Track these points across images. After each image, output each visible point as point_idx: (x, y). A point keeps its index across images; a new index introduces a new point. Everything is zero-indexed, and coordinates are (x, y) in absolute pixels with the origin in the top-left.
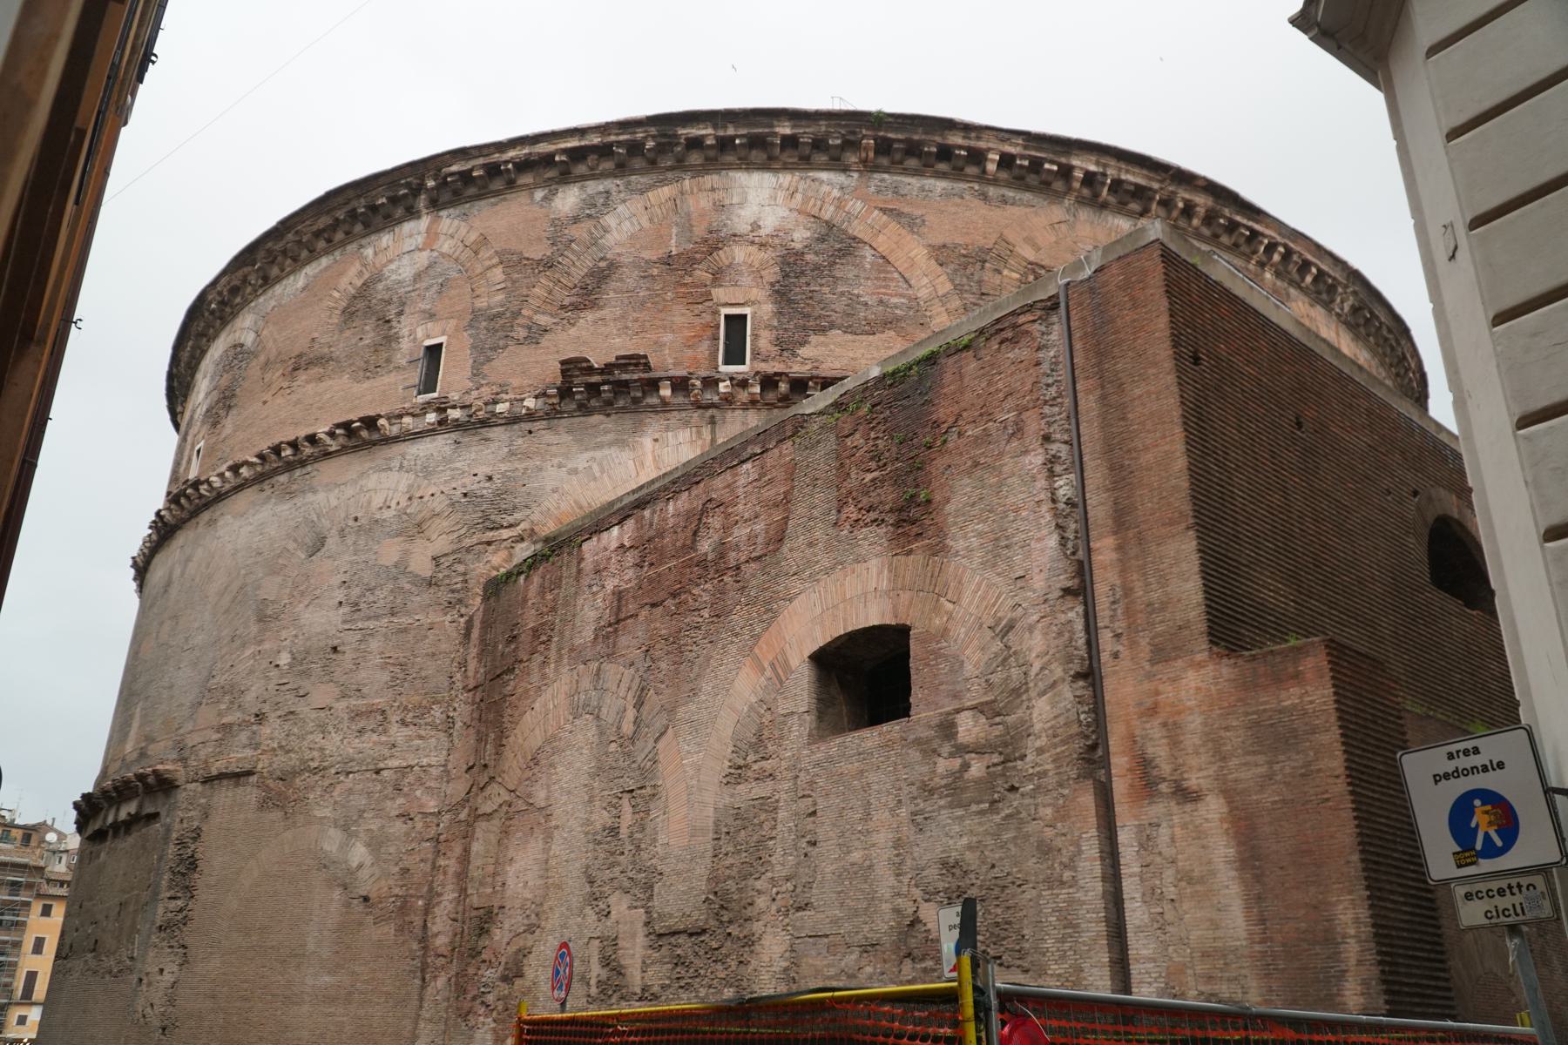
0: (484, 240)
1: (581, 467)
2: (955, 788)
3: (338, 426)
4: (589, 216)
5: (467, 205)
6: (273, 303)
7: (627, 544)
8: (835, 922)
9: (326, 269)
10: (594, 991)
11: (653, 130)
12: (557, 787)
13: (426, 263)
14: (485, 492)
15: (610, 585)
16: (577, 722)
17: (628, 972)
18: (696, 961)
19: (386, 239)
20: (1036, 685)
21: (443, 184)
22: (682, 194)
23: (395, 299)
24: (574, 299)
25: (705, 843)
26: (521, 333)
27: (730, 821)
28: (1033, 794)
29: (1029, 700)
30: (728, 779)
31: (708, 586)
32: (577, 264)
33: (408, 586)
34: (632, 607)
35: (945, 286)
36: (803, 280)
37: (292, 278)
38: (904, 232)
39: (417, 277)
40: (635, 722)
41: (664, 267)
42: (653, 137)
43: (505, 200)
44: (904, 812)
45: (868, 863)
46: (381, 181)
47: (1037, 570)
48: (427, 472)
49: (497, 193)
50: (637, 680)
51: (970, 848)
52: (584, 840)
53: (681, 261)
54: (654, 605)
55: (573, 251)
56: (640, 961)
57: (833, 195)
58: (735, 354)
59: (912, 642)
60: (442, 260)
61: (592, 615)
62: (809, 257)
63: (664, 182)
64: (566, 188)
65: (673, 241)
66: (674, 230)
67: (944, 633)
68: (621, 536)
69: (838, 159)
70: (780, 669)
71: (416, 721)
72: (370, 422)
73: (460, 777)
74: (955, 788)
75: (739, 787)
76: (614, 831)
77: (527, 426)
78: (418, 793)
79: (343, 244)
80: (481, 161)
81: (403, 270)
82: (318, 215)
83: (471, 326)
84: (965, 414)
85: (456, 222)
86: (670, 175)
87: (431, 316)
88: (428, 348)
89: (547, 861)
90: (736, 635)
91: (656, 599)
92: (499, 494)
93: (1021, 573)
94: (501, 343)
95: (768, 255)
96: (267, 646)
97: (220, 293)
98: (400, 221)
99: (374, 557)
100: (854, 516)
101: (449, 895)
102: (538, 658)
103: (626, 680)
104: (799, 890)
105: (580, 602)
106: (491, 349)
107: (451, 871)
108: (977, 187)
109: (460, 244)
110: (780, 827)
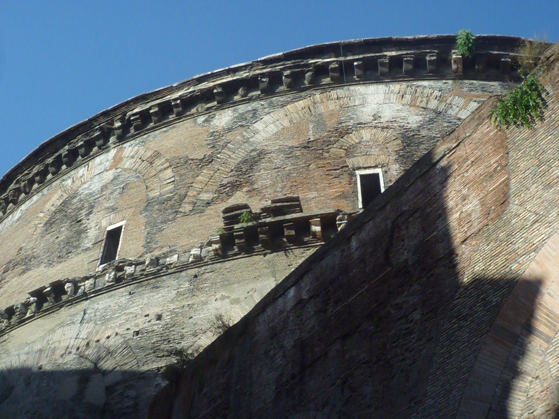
0: (157, 155)
1: (242, 297)
3: (33, 294)
7: (305, 297)
11: (289, 63)
13: (111, 177)
14: (155, 327)
15: (289, 343)
21: (127, 125)
23: (86, 205)
24: (230, 179)
26: (187, 207)
32: (233, 156)
37: (11, 216)
39: (104, 187)
41: (305, 151)
43: (174, 127)
48: (105, 320)
55: (229, 149)
62: (424, 132)
64: (222, 112)
65: (311, 132)
66: (311, 126)
68: (298, 292)
77: (193, 272)
81: (96, 186)
83: (145, 210)
85: (136, 148)
87: (113, 209)
88: (110, 232)
90: (465, 318)
106: (162, 223)
109: (139, 161)
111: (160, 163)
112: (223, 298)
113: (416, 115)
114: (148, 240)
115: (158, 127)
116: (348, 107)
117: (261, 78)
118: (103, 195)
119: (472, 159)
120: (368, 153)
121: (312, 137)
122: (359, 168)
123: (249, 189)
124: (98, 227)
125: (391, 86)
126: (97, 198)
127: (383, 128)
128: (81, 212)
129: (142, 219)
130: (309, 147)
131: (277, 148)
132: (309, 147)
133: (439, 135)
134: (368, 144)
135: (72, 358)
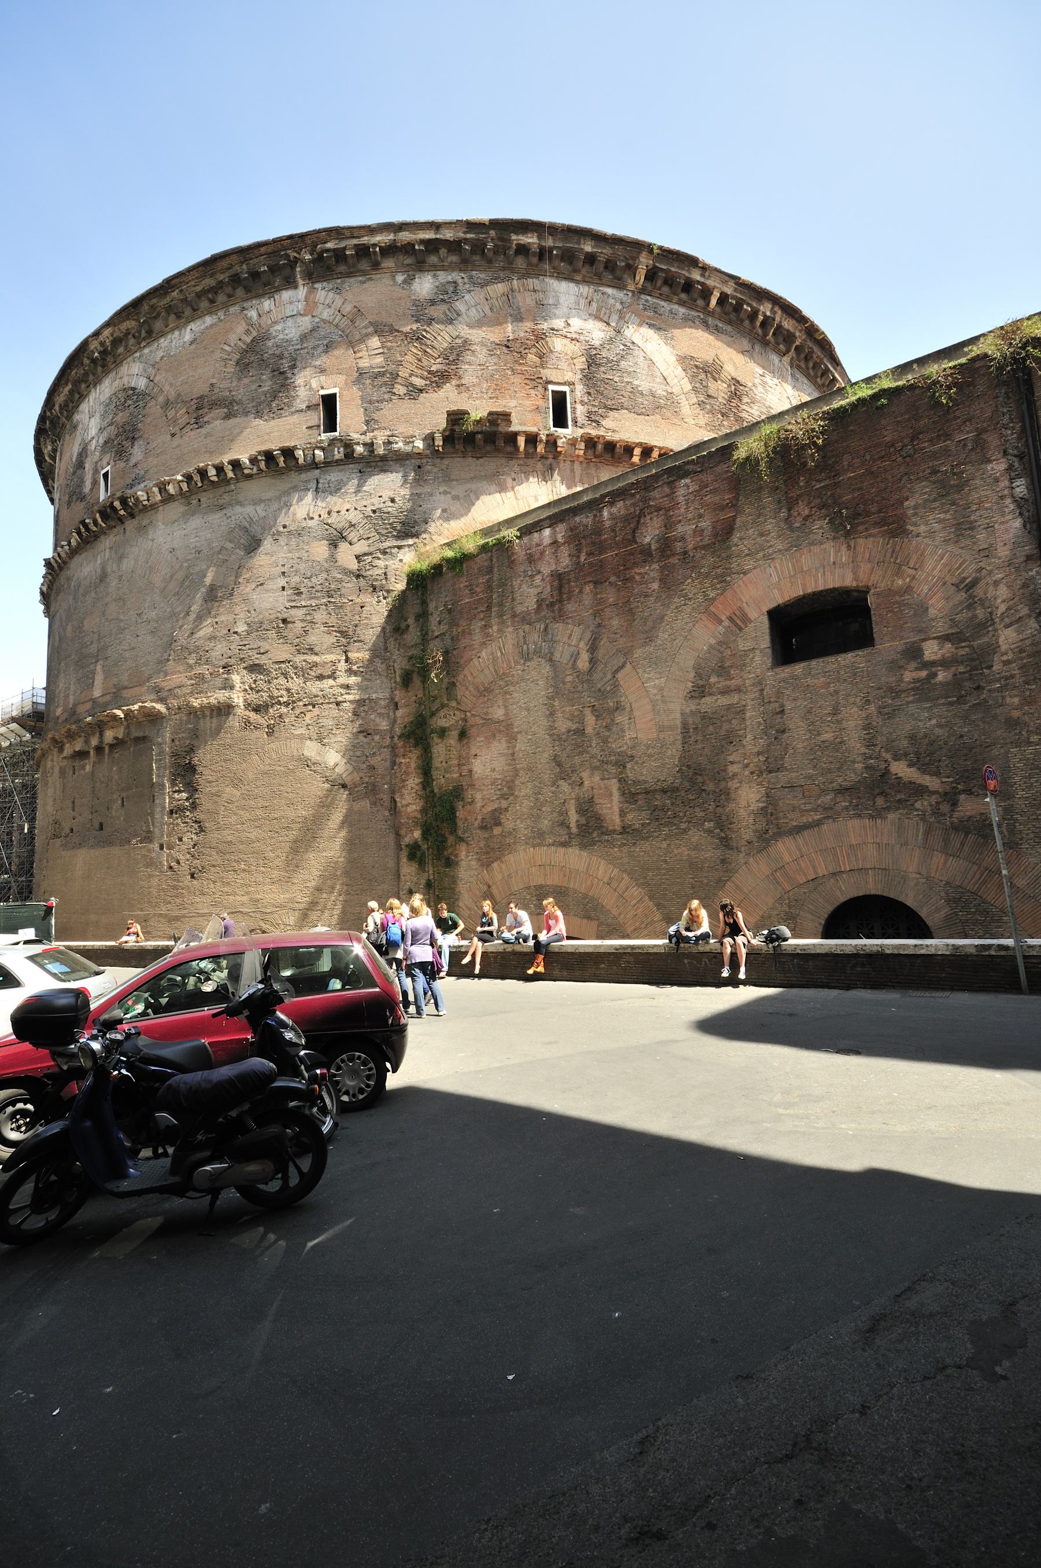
1: (461, 495)
2: (923, 690)
3: (259, 453)
4: (443, 300)
5: (339, 281)
6: (160, 354)
9: (212, 326)
10: (574, 830)
12: (515, 707)
13: (310, 327)
14: (390, 509)
15: (546, 570)
16: (528, 663)
19: (267, 304)
20: (1002, 620)
21: (319, 259)
22: (513, 291)
23: (286, 354)
24: (439, 367)
25: (675, 736)
27: (698, 720)
28: (1000, 690)
29: (996, 630)
30: (692, 694)
31: (655, 566)
33: (339, 576)
35: (688, 387)
36: (602, 369)
37: (177, 333)
38: (662, 344)
39: (304, 338)
40: (590, 662)
43: (371, 279)
44: (872, 708)
45: (838, 740)
46: (263, 250)
47: (1002, 544)
49: (364, 273)
50: (588, 635)
51: (940, 726)
57: (616, 308)
58: (560, 420)
60: (322, 324)
61: (533, 591)
63: (497, 280)
67: (908, 589)
69: (619, 279)
70: (739, 621)
72: (288, 453)
74: (923, 690)
76: (580, 732)
78: (372, 717)
79: (226, 306)
80: (355, 241)
82: (203, 276)
85: (331, 294)
89: (513, 754)
90: (690, 599)
94: (386, 396)
96: (221, 618)
97: (102, 344)
98: (278, 290)
99: (306, 555)
101: (414, 782)
105: (516, 583)
107: (413, 765)
108: (702, 317)
109: (337, 312)
112: (445, 493)
115: (352, 273)
118: (305, 348)
121: (511, 335)
122: (551, 382)
123: (457, 383)
126: (298, 350)
130: (508, 347)
131: (480, 340)
132: (508, 347)
133: (615, 359)
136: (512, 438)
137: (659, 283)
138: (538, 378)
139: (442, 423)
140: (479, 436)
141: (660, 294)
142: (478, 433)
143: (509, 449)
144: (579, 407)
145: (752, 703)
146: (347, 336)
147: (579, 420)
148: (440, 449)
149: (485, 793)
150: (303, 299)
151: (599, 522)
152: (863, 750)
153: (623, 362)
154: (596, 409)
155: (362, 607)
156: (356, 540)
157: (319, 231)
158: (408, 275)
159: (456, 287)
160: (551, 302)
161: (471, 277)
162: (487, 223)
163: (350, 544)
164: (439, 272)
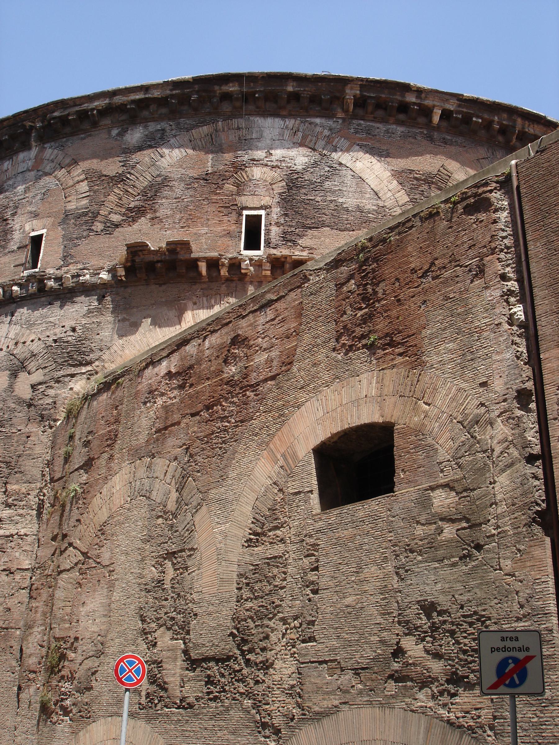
7: (173, 371)
8: (333, 650)
10: (143, 700)
11: (197, 87)
14: (70, 338)
17: (170, 686)
18: (223, 680)
23: (11, 205)
24: (137, 203)
26: (99, 226)
33: (13, 406)
34: (176, 417)
40: (177, 501)
42: (197, 92)
43: (90, 135)
44: (390, 567)
46: (5, 123)
49: (85, 131)
50: (180, 470)
52: (138, 589)
53: (216, 177)
54: (193, 415)
56: (179, 679)
57: (324, 134)
59: (396, 435)
63: (204, 123)
71: (15, 502)
73: (48, 543)
75: (256, 549)
78: (17, 554)
80: (77, 108)
84: (437, 262)
85: (56, 151)
86: (208, 118)
87: (36, 215)
88: (33, 238)
91: (194, 411)
92: (80, 340)
93: (484, 379)
94: (85, 234)
95: (276, 174)
98: (17, 152)
100: (349, 343)
102: (106, 456)
103: (171, 470)
104: (304, 626)
106: (77, 238)
107: (40, 610)
108: (425, 132)
109: (57, 166)
110: (289, 579)
111: (77, 173)
113: (304, 156)
114: (65, 254)
116: (246, 140)
117: (171, 98)
119: (282, 316)
120: (256, 193)
121: (210, 169)
122: (247, 208)
123: (152, 216)
124: (22, 230)
125: (287, 120)
126: (21, 199)
127: (273, 167)
128: (6, 210)
129: (60, 231)
130: (206, 180)
131: (179, 176)
132: (206, 180)
133: (319, 181)
134: (257, 183)
135: (3, 355)
136: (194, 264)
137: (370, 108)
138: (232, 205)
139: (121, 253)
140: (159, 265)
141: (374, 118)
142: (158, 262)
143: (192, 274)
144: (275, 230)
145: (294, 556)
146: (61, 185)
147: (273, 240)
148: (123, 278)
149: (85, 648)
150: (34, 158)
151: (201, 352)
152: (379, 620)
153: (327, 183)
154: (293, 229)
155: (28, 437)
156: (34, 369)
157: (48, 105)
158: (122, 129)
159: (163, 134)
160: (254, 136)
161: (179, 124)
162: (191, 80)
163: (29, 374)
164: (149, 123)
